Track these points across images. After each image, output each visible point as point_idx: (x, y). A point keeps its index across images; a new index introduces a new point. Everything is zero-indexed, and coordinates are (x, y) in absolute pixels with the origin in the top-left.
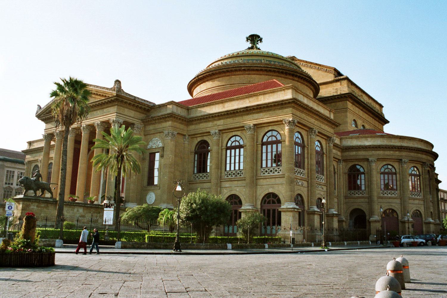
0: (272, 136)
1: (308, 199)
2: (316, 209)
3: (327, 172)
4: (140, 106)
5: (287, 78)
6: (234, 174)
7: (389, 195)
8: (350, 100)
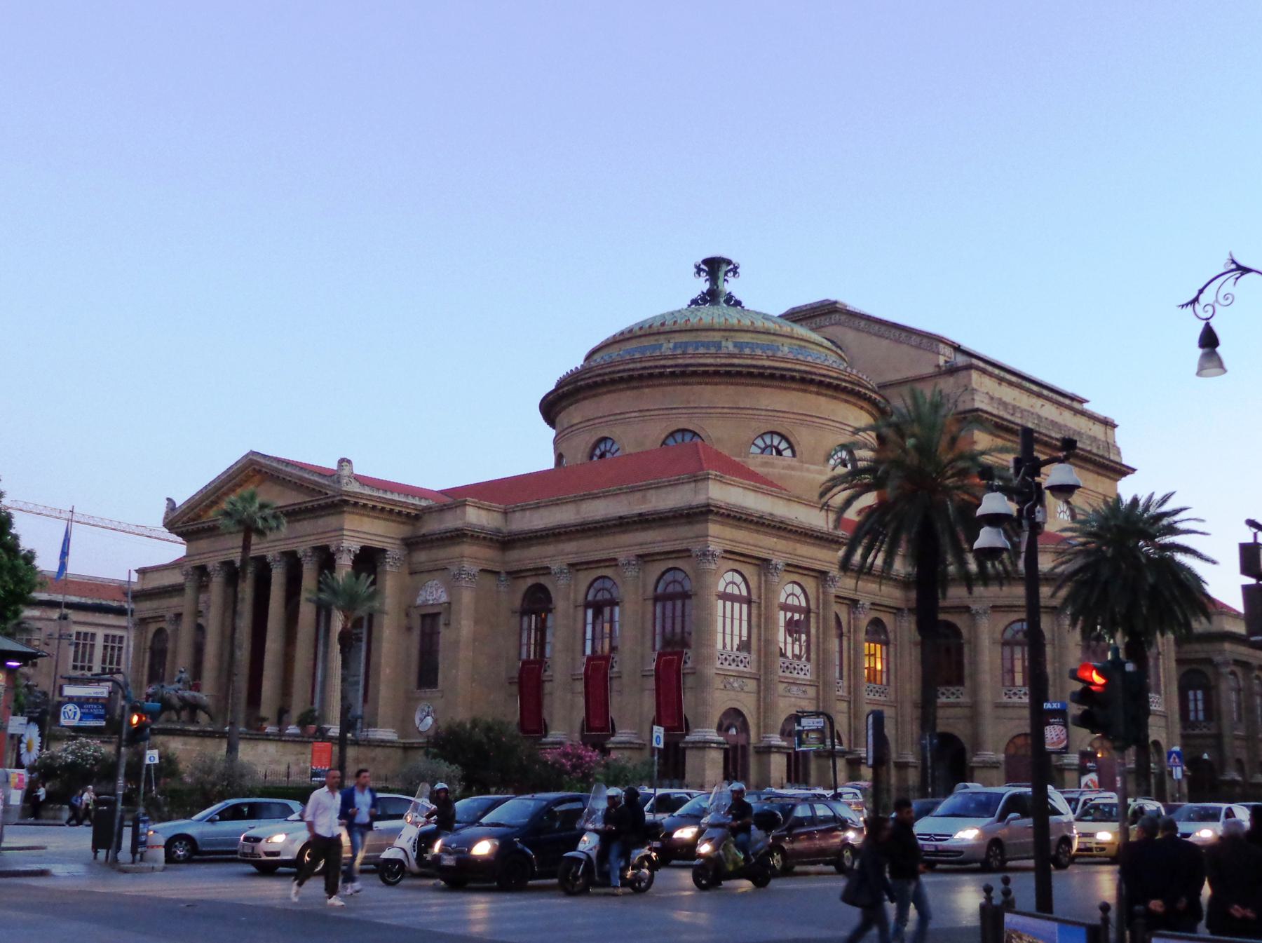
2: (776, 740)
3: (818, 655)
4: (397, 509)
5: (785, 388)
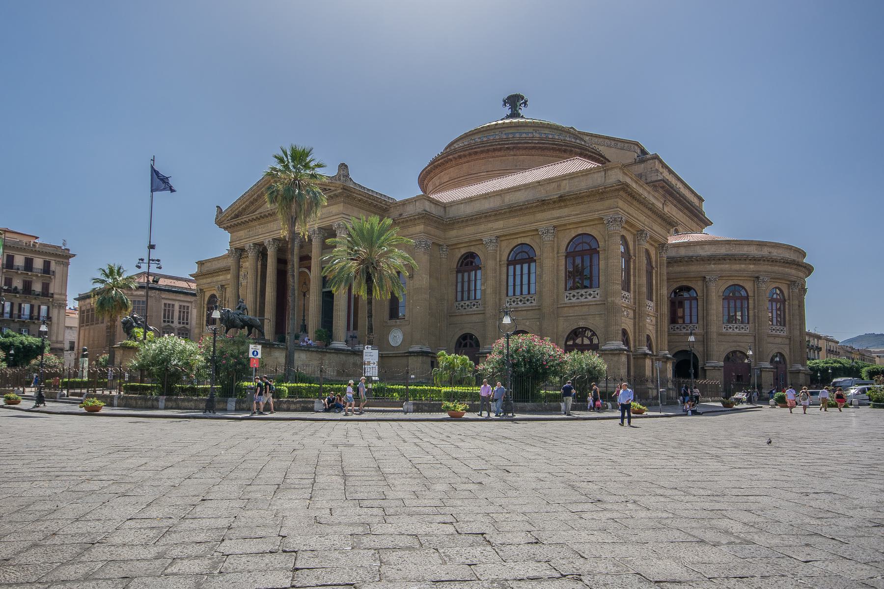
0: (582, 243)
1: (635, 336)
6: (521, 301)
7: (737, 331)
8: (660, 190)
